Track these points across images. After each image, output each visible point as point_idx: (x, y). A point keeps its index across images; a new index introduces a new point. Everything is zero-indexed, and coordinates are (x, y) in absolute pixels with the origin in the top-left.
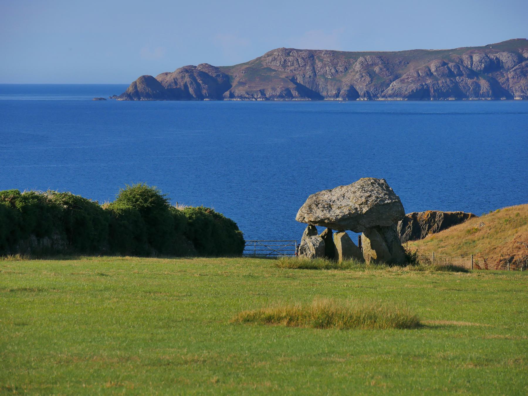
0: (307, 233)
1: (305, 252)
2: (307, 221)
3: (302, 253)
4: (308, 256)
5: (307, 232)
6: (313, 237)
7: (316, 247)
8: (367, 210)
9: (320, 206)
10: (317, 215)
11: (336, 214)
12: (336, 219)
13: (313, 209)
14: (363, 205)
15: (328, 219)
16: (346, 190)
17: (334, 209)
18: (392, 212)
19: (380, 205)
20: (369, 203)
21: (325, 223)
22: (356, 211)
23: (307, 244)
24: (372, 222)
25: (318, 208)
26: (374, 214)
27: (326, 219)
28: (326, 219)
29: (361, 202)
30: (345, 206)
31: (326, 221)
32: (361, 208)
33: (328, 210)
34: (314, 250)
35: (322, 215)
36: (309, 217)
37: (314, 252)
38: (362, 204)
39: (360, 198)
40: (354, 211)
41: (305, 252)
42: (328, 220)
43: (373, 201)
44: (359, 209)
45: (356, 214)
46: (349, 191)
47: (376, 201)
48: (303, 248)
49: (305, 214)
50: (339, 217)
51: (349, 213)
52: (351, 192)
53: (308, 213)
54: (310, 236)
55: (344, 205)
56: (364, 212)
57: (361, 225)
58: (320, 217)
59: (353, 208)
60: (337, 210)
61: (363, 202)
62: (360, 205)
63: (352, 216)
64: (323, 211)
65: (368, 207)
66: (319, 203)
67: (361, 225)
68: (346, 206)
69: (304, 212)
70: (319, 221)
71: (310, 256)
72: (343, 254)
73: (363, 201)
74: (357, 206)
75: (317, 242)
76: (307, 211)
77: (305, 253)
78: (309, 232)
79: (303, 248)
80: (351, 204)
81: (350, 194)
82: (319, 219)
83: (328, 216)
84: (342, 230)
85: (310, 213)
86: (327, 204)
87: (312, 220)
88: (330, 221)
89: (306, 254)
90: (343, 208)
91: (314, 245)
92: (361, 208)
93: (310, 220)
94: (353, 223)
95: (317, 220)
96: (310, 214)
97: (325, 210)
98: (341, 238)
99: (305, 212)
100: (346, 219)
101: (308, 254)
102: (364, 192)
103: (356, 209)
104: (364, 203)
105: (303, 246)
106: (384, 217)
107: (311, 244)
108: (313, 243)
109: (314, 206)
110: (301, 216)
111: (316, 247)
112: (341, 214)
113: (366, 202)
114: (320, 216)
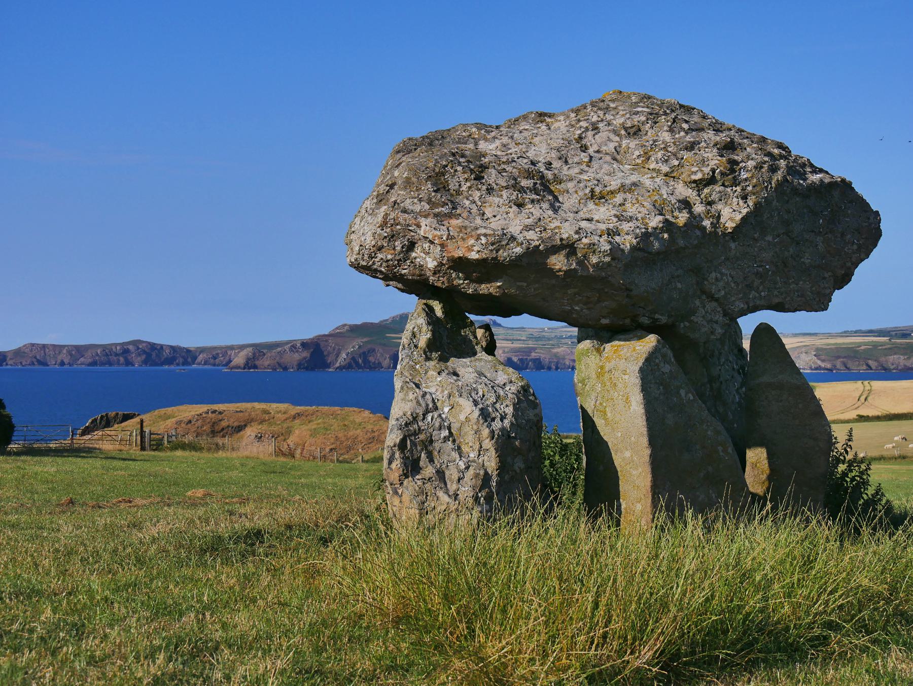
0: (423, 341)
1: (431, 461)
2: (431, 264)
3: (412, 468)
4: (452, 487)
5: (424, 338)
6: (466, 368)
7: (497, 425)
8: (745, 211)
9: (491, 176)
10: (496, 224)
11: (603, 227)
12: (615, 251)
13: (458, 192)
14: (718, 188)
15: (569, 248)
16: (584, 124)
17: (568, 202)
18: (843, 235)
19: (795, 191)
20: (744, 175)
21: (551, 272)
22: (690, 212)
23: (436, 408)
24: (757, 282)
25: (490, 190)
26: (769, 238)
27: (554, 250)
28: (554, 250)
29: (707, 170)
30: (623, 188)
31: (558, 262)
32: (710, 203)
33: (545, 205)
34: (488, 444)
35: (528, 228)
36: (450, 237)
37: (491, 462)
38: (711, 181)
39: (686, 155)
40: (682, 218)
41: (431, 461)
42: (568, 256)
43: (758, 167)
44: (699, 209)
45: (698, 233)
46: (601, 125)
47: (773, 169)
48: (415, 434)
49: (423, 222)
50: (627, 241)
51: (668, 225)
52: (615, 132)
53: (436, 215)
54: (444, 359)
55: (614, 184)
56: (730, 225)
57: (712, 298)
58: (520, 238)
59: (673, 200)
60: (591, 205)
61: (713, 171)
62: (699, 185)
63: (681, 243)
64: (520, 205)
65: (745, 198)
66: (484, 168)
67: (712, 298)
68: (630, 191)
69: (408, 204)
70: (519, 257)
71: (466, 491)
72: (658, 464)
73: (713, 163)
74: (683, 191)
75: (498, 397)
76: (429, 202)
77: (429, 471)
78: (434, 332)
79: (415, 434)
80: (647, 182)
81: (609, 140)
82: (519, 250)
83: (567, 231)
84: (628, 321)
85: (450, 216)
86: (529, 175)
87: (474, 256)
88: (580, 263)
89: (441, 474)
90: (619, 199)
91: (485, 415)
92: (710, 203)
93: (459, 253)
94: (679, 285)
95: (503, 254)
96: (454, 222)
97: (533, 201)
98: (641, 370)
99: (417, 208)
100: (658, 253)
101: (452, 474)
102: (685, 126)
103: (686, 204)
104: (723, 174)
105: (415, 419)
106: (807, 260)
107: (467, 410)
108: (476, 403)
109: (459, 179)
110: (392, 237)
111: (497, 425)
112: (626, 226)
113: (733, 171)
114: (514, 229)
